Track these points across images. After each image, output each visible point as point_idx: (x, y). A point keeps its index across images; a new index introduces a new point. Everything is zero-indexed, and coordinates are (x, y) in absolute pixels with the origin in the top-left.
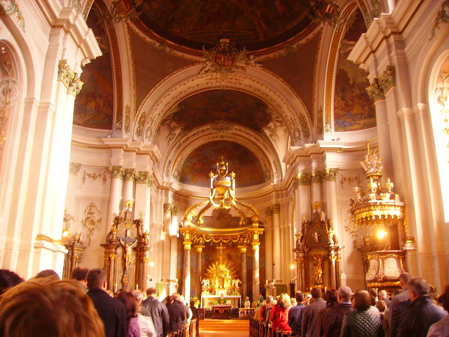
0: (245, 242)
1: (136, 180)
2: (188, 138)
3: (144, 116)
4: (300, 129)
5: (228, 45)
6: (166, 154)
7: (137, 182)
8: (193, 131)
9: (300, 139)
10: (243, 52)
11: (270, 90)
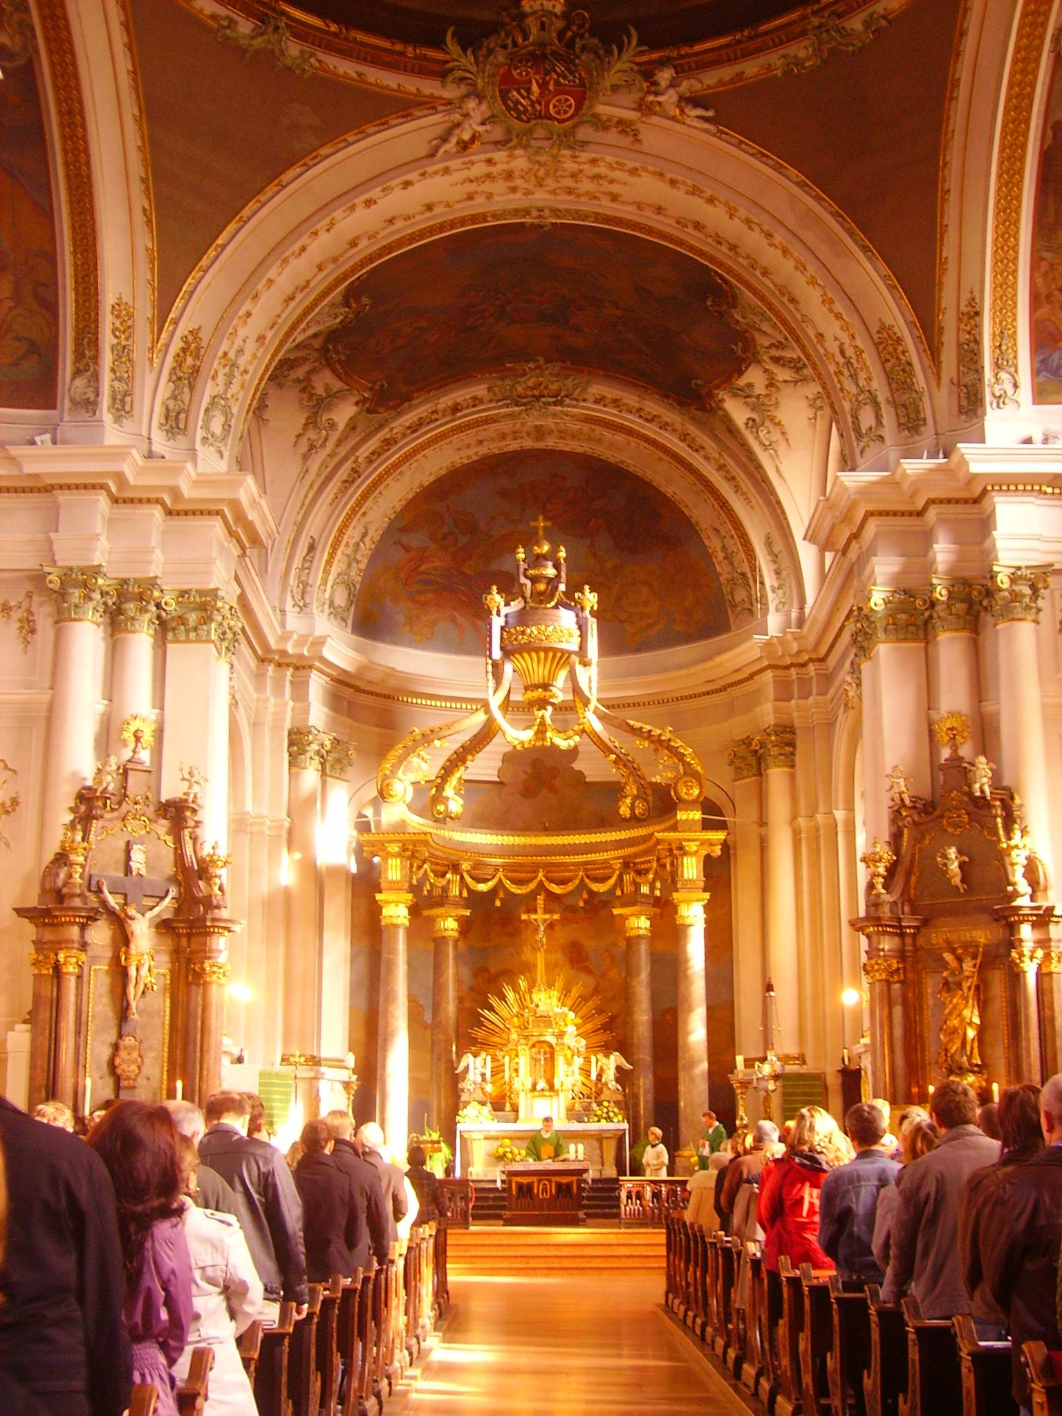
0: (645, 889)
1: (165, 629)
2: (388, 443)
3: (193, 346)
4: (881, 398)
5: (559, 24)
6: (293, 515)
7: (170, 636)
8: (411, 408)
9: (881, 438)
10: (625, 57)
11: (748, 222)
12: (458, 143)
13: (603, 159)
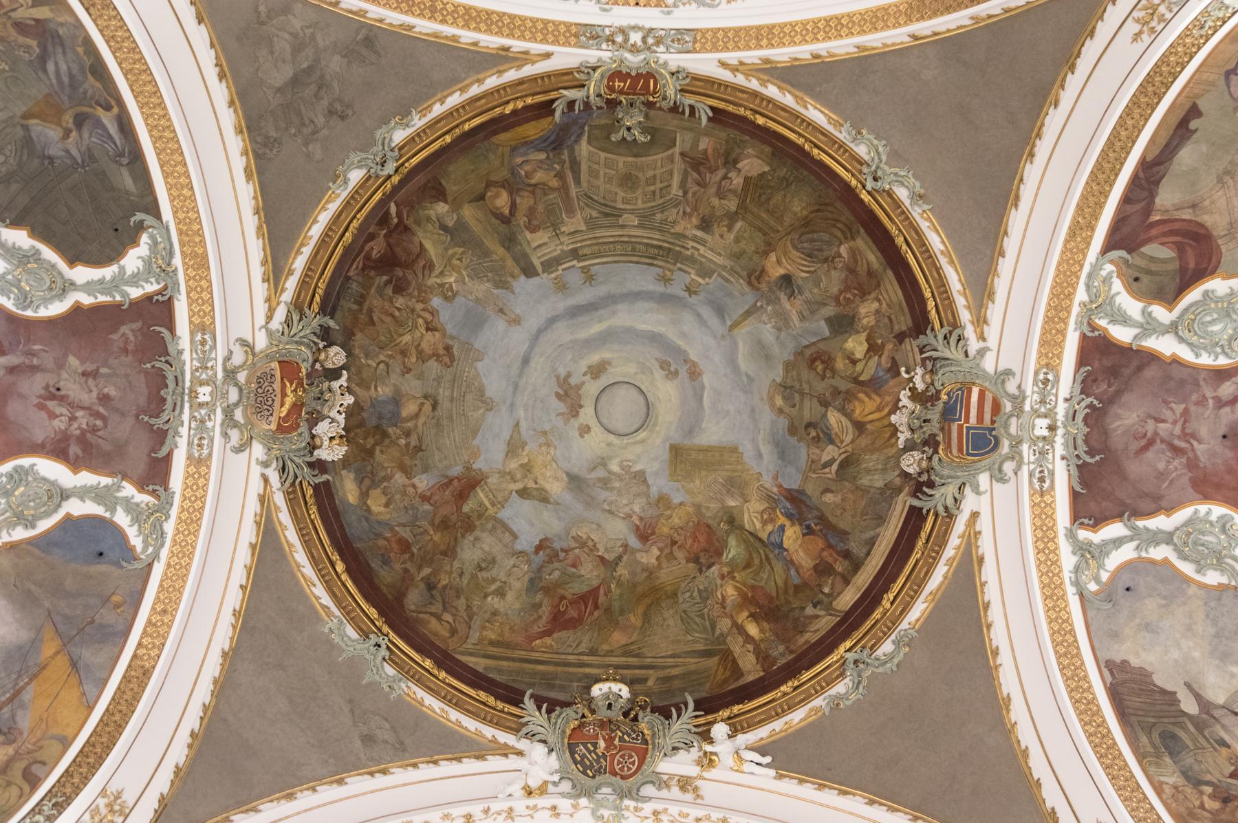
12: (523, 788)
13: (666, 810)
